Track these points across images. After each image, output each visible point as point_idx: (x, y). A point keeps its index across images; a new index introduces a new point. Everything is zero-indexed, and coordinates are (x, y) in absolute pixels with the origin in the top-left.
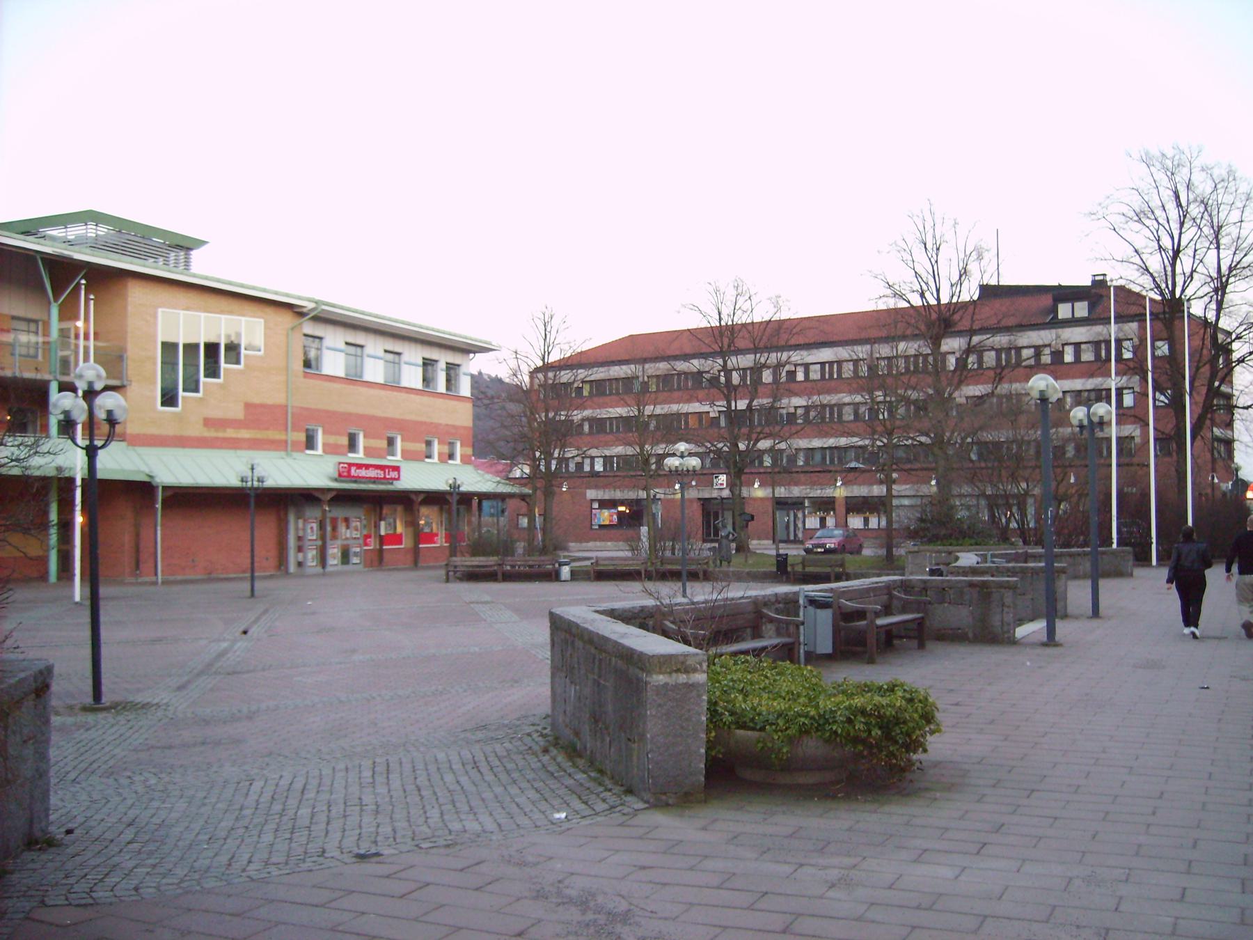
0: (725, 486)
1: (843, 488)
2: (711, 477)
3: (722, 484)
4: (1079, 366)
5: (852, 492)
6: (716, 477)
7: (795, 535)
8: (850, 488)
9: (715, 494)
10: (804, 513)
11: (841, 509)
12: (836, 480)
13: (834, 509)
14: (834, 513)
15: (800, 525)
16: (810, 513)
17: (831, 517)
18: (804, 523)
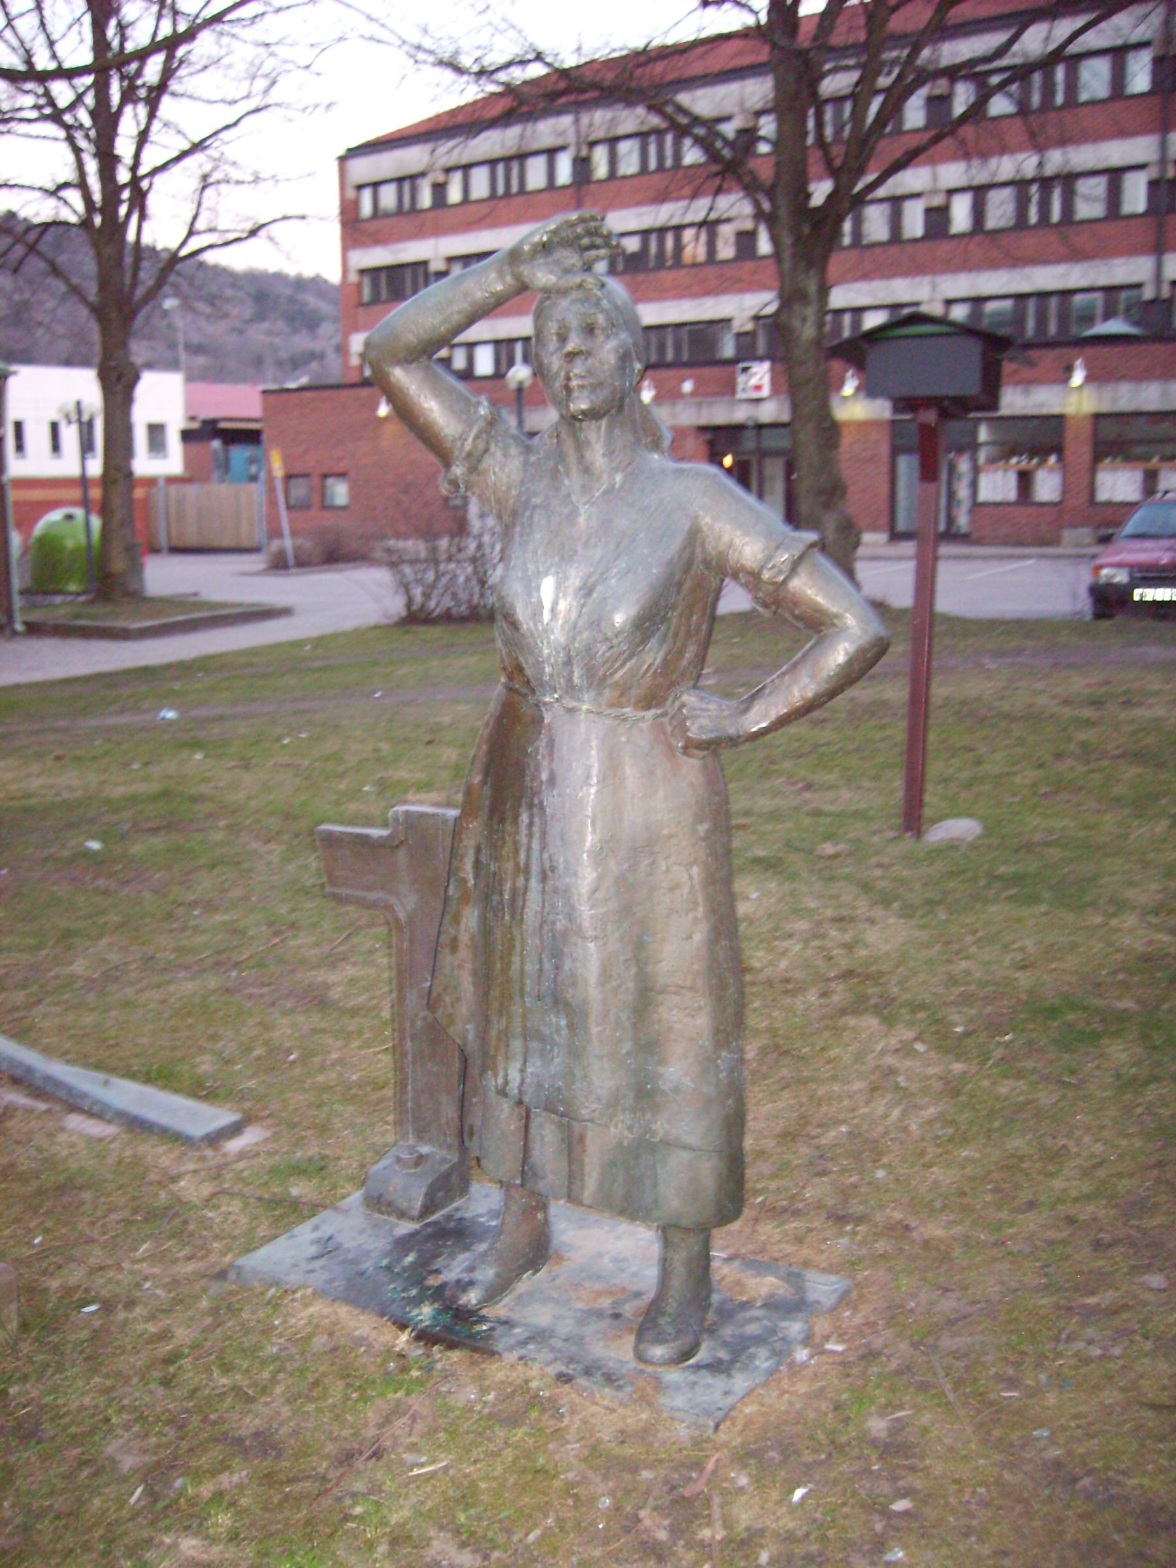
0: (765, 392)
1: (1087, 392)
2: (730, 369)
3: (758, 388)
4: (1118, 106)
5: (1115, 400)
6: (745, 370)
7: (950, 520)
8: (1108, 391)
9: (740, 415)
10: (974, 460)
11: (1079, 447)
12: (1069, 370)
13: (1058, 450)
14: (1060, 459)
15: (963, 492)
16: (992, 461)
17: (1051, 470)
18: (974, 486)
